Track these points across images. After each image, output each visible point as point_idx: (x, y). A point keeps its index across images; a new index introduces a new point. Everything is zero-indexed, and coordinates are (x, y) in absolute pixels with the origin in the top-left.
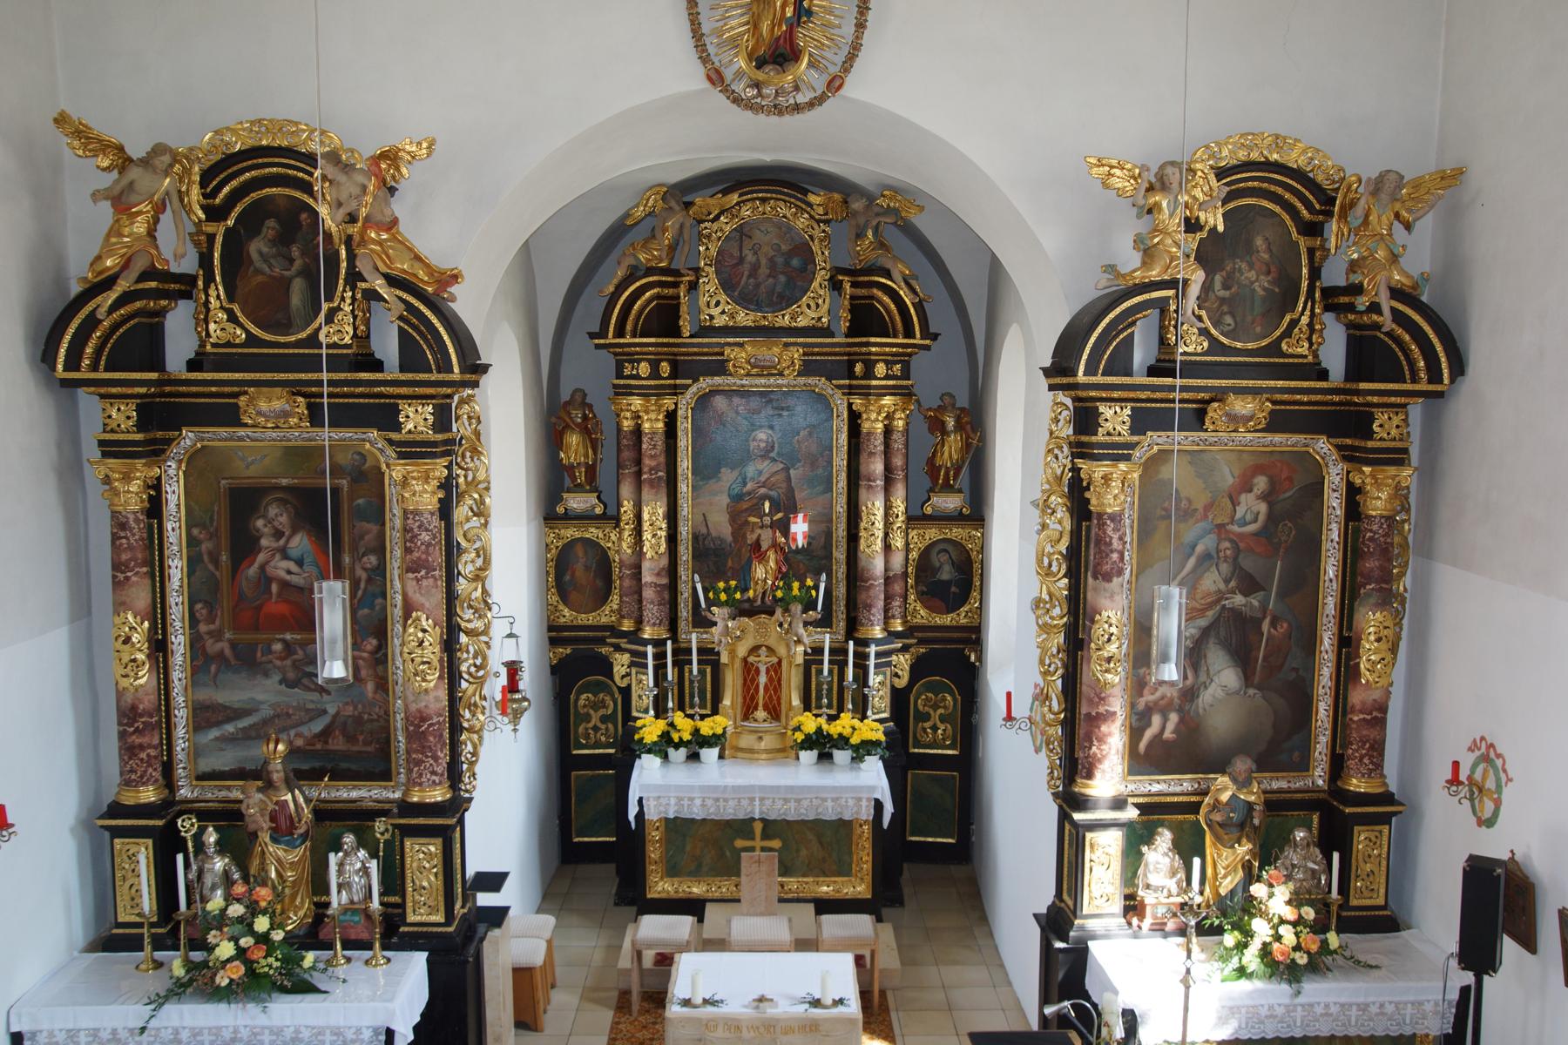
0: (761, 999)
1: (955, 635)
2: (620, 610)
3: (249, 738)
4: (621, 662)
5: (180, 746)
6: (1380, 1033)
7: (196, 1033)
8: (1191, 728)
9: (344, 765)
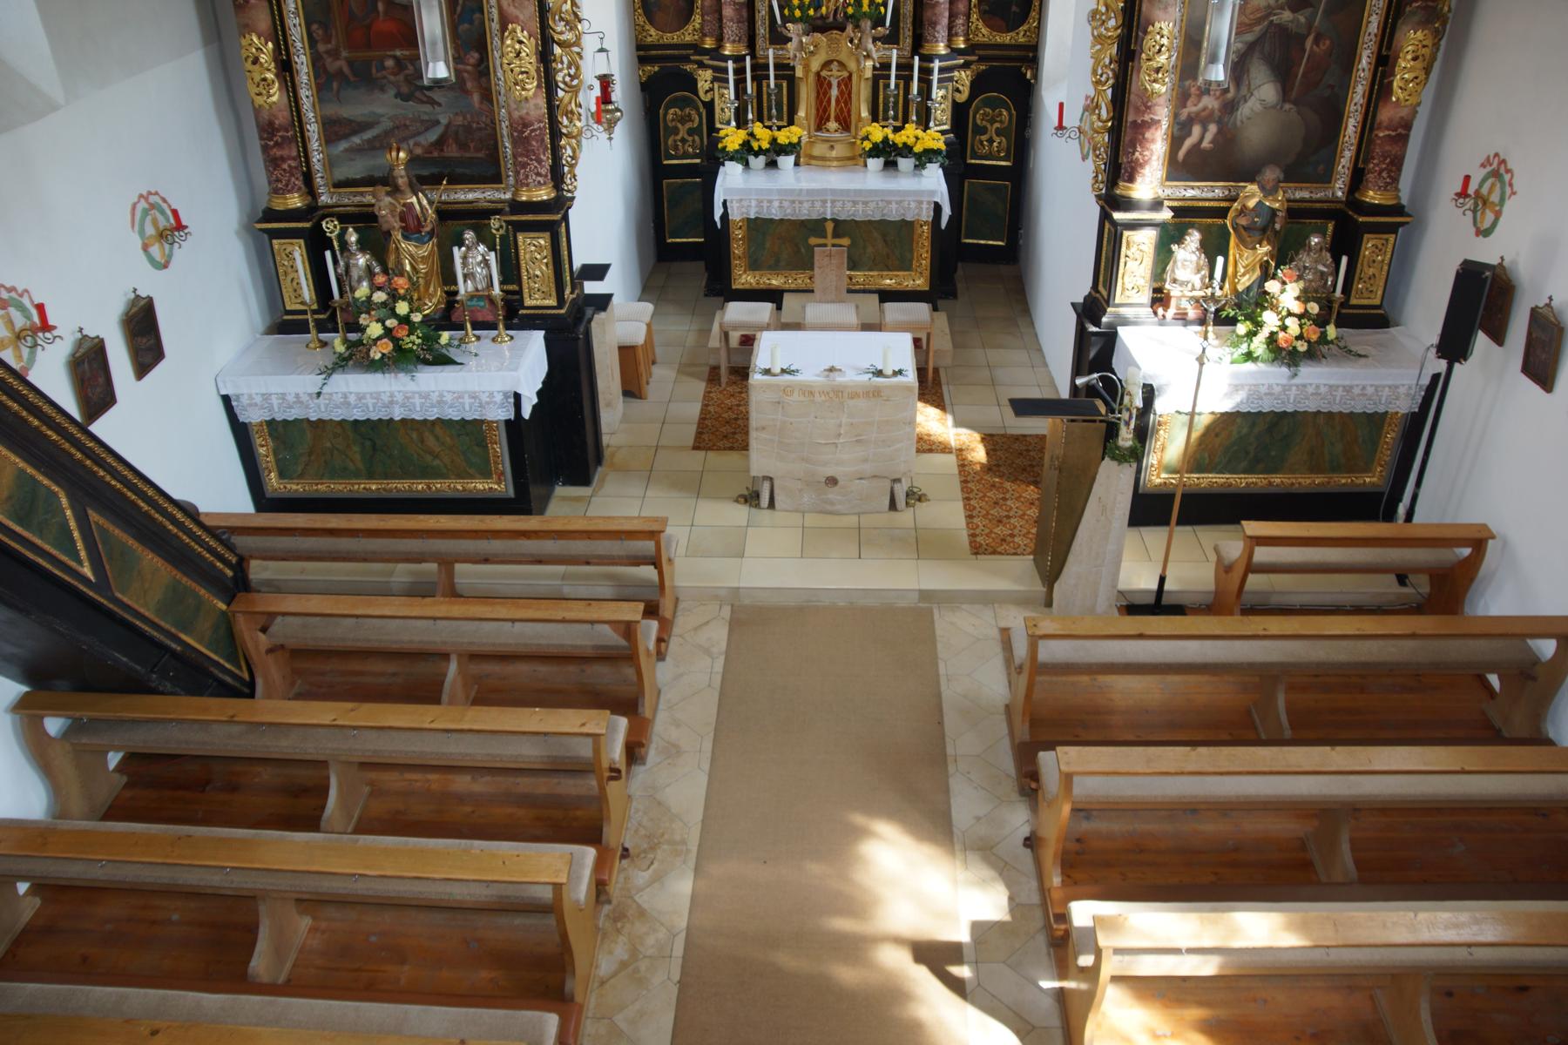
0: (832, 370)
1: (1013, 53)
2: (702, 29)
3: (373, 148)
4: (704, 78)
5: (316, 157)
6: (1358, 410)
7: (361, 397)
8: (1227, 138)
9: (459, 170)
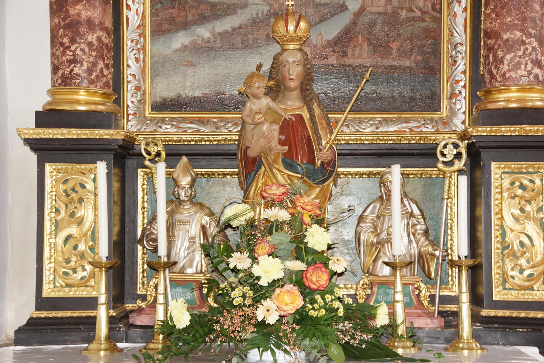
3: (232, 47)
